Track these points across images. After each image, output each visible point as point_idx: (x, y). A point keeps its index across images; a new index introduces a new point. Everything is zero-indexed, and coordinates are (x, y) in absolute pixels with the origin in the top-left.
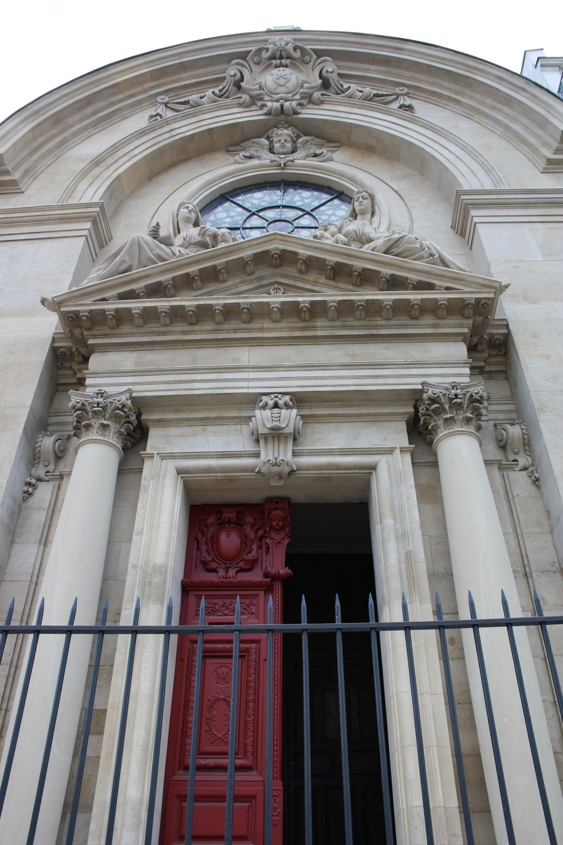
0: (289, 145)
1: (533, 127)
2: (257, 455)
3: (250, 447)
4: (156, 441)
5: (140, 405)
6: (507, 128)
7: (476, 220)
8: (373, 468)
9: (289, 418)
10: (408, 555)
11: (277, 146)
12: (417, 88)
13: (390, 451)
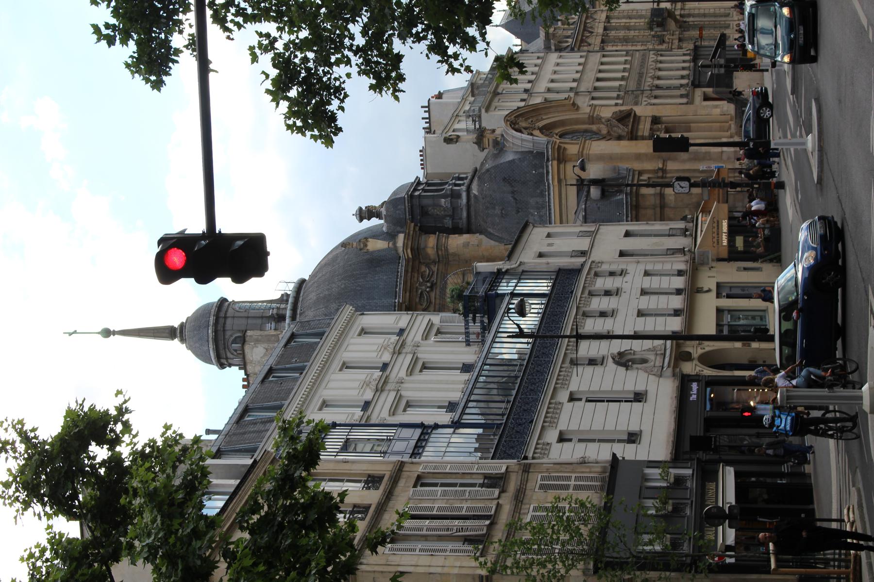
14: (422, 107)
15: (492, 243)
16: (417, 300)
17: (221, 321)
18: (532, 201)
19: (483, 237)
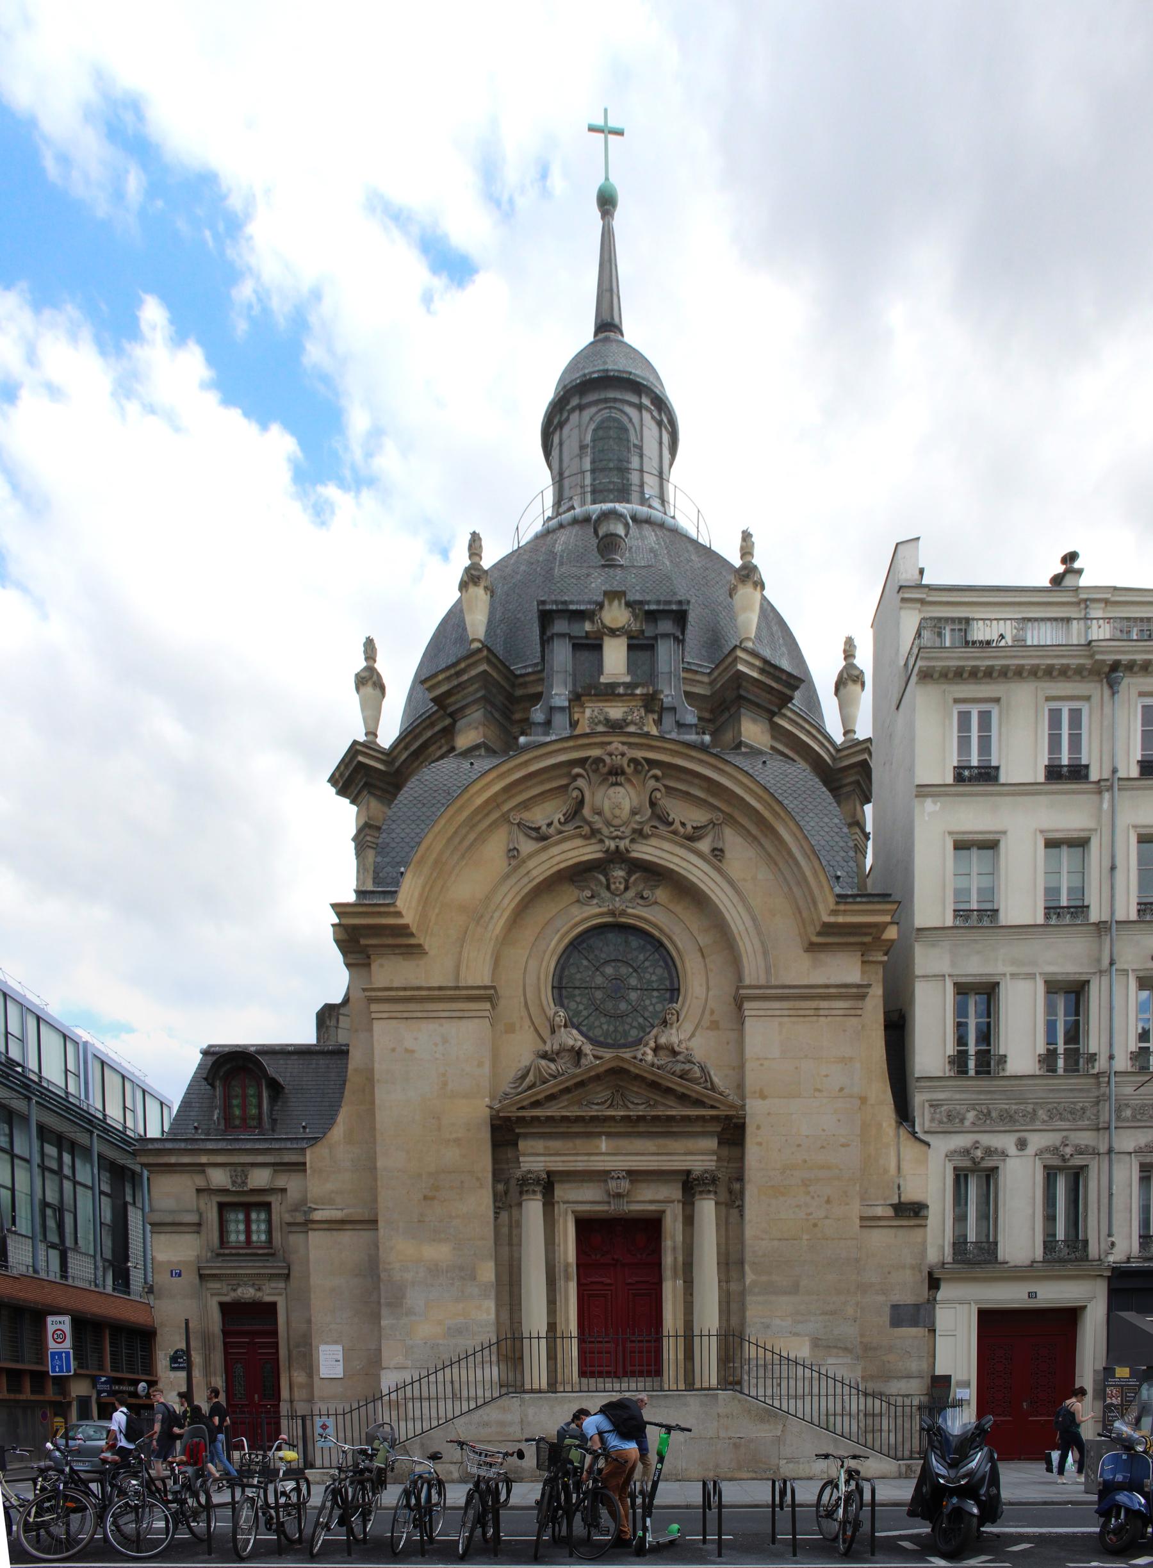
0: (622, 887)
2: (609, 1203)
3: (606, 1199)
4: (559, 1192)
5: (549, 1173)
8: (664, 1212)
9: (625, 1185)
10: (675, 1258)
11: (613, 887)
13: (673, 1202)
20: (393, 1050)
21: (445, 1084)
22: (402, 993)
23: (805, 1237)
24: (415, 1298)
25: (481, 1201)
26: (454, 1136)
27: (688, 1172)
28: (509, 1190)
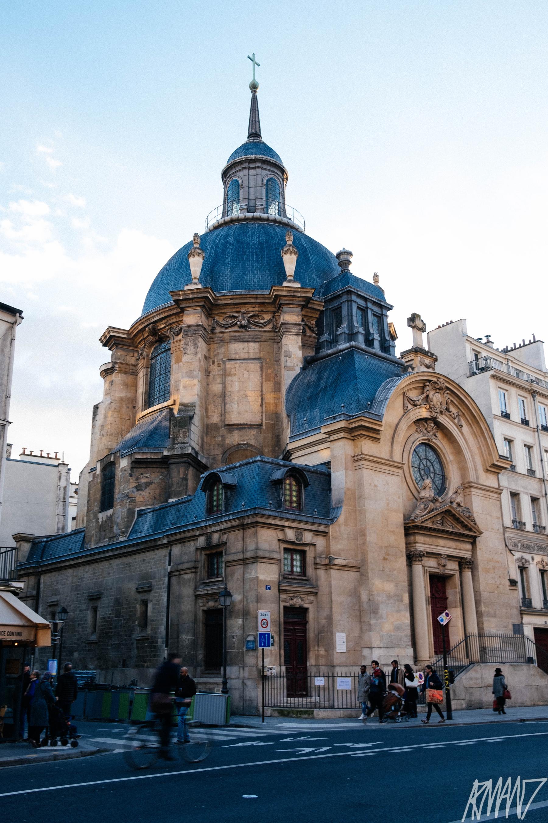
1: (487, 452)
6: (480, 446)
7: (472, 493)
8: (455, 575)
12: (463, 414)
14: (534, 337)
15: (290, 381)
16: (228, 314)
17: (252, 165)
18: (316, 412)
19: (298, 371)
20: (371, 484)
21: (388, 504)
22: (375, 459)
23: (496, 592)
24: (383, 610)
25: (403, 561)
26: (392, 530)
27: (462, 558)
28: (412, 558)
